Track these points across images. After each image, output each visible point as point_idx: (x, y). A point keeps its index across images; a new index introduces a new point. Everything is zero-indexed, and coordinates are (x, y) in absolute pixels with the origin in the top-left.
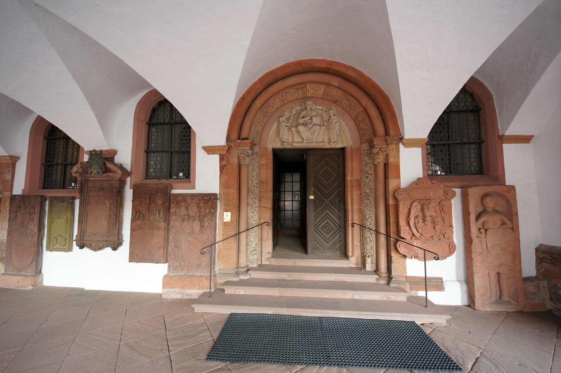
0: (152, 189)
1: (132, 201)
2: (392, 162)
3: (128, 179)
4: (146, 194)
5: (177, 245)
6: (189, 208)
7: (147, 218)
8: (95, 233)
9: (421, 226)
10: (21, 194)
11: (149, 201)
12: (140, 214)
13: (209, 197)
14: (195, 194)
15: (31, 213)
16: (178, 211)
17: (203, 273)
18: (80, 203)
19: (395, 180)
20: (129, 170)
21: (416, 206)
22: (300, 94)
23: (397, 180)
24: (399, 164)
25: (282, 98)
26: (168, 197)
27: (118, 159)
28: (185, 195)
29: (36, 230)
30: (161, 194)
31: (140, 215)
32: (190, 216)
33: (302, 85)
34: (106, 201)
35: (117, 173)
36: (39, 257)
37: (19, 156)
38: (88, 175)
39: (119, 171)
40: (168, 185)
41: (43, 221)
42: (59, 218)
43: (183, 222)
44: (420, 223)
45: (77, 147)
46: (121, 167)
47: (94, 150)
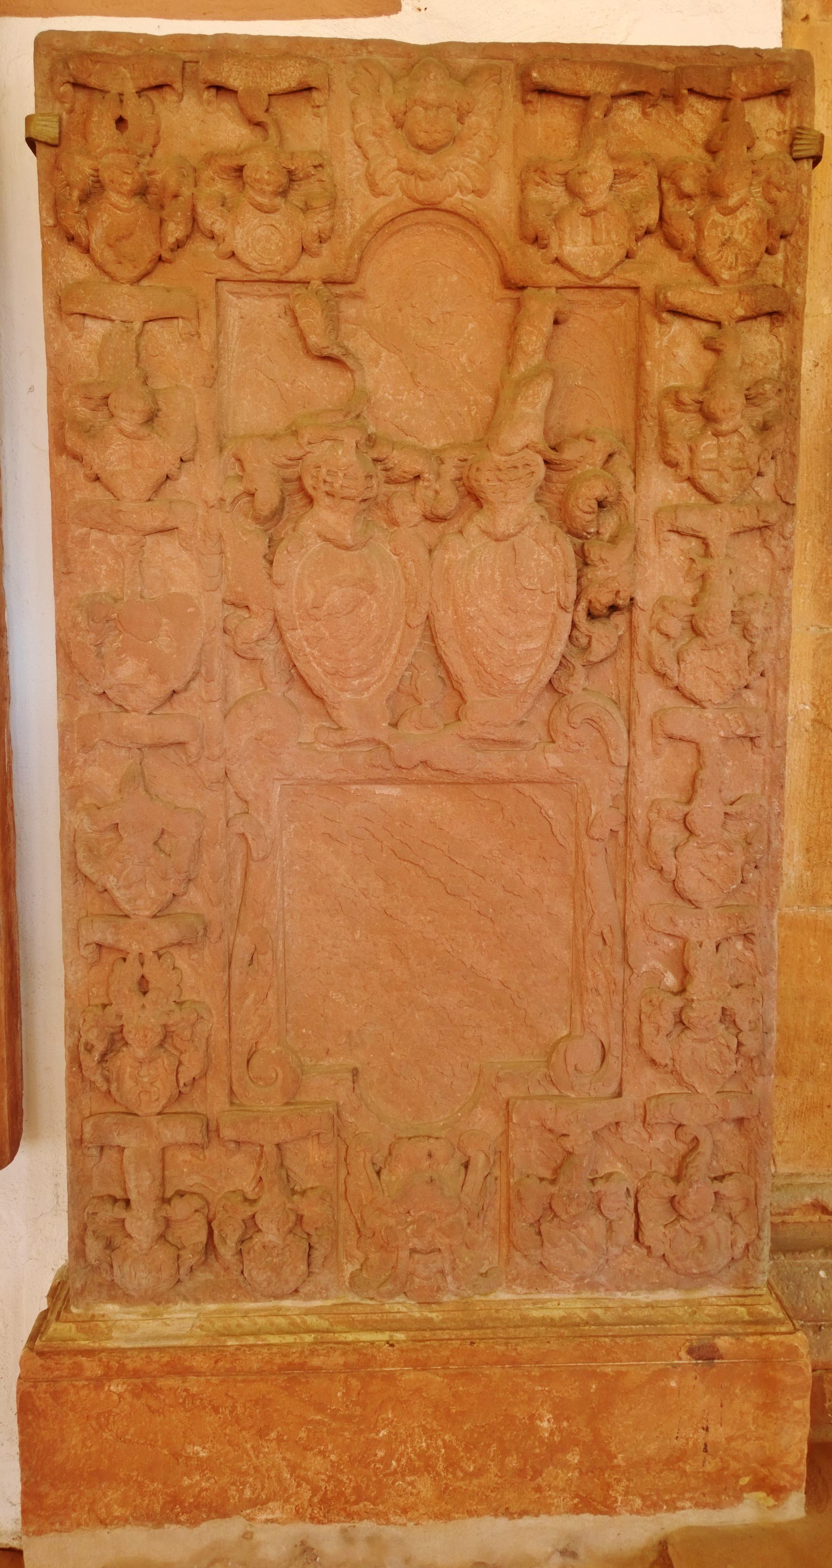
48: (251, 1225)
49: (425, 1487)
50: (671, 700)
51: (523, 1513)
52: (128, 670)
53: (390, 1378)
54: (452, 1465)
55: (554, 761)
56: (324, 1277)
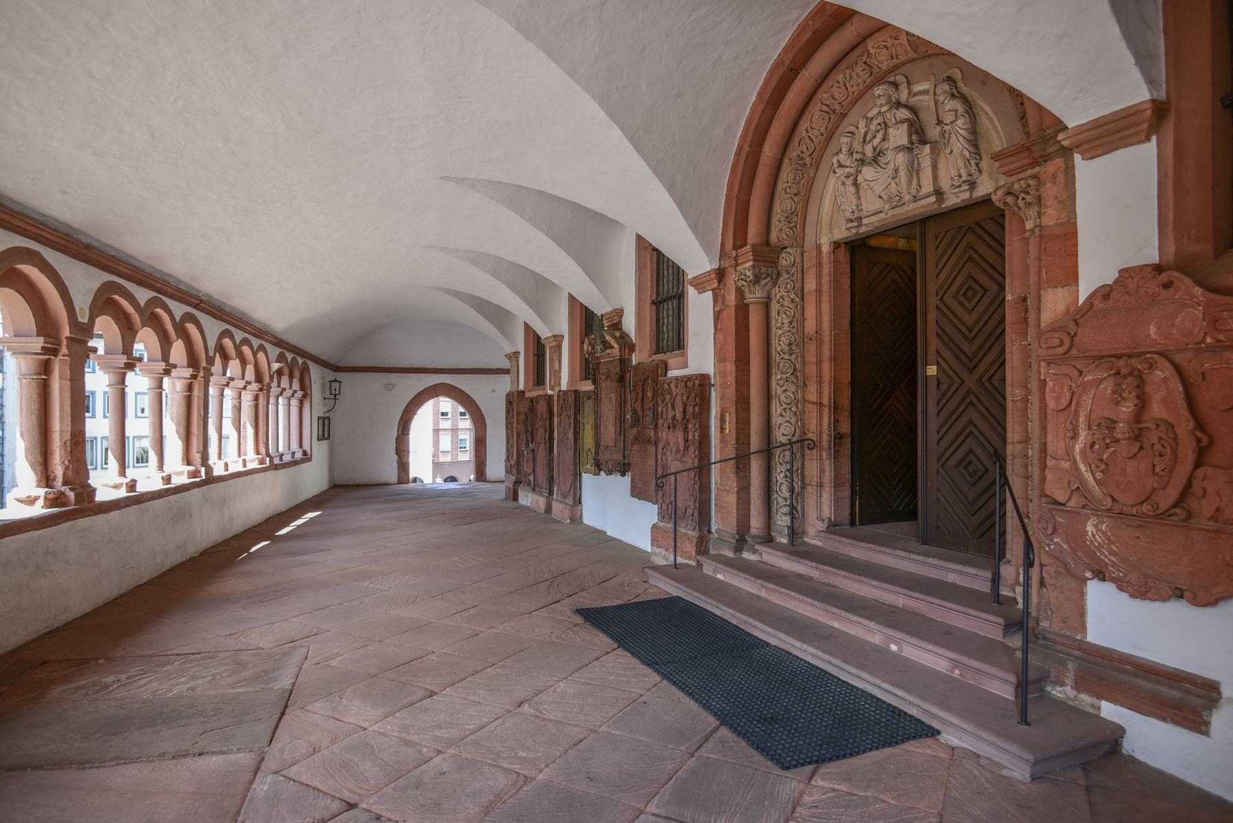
2: (1052, 223)
9: (1105, 457)
19: (1060, 289)
21: (1101, 381)
22: (860, 75)
23: (1066, 288)
24: (1075, 224)
25: (824, 108)
33: (859, 50)
44: (1097, 447)
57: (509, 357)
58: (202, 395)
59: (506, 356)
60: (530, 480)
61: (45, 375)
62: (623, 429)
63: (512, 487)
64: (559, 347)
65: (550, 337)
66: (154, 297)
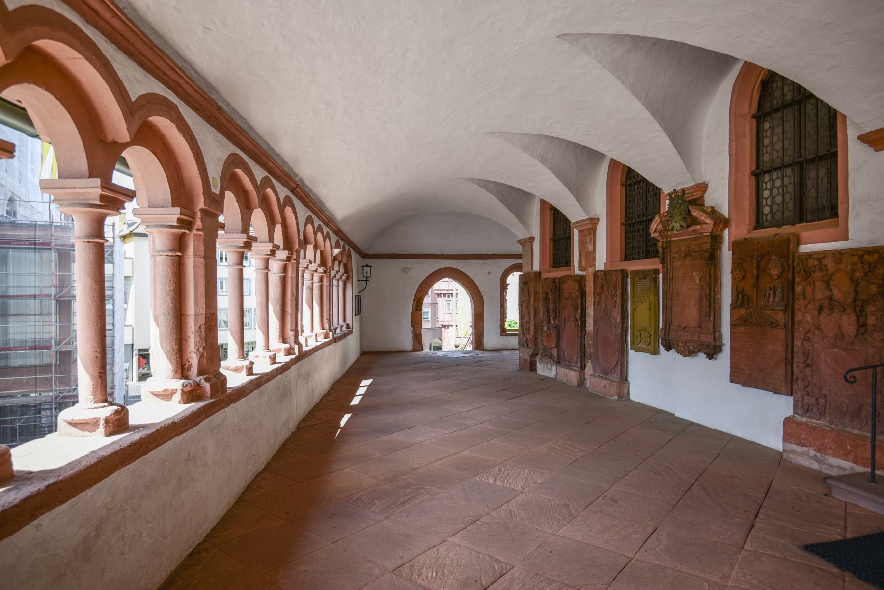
0: (762, 247)
1: (731, 273)
3: (726, 233)
4: (752, 257)
5: (809, 361)
6: (831, 283)
7: (755, 303)
8: (682, 328)
10: (603, 269)
11: (758, 271)
12: (744, 296)
13: (876, 256)
14: (845, 251)
15: (613, 295)
16: (809, 289)
17: (865, 432)
18: (663, 278)
20: (727, 216)
26: (790, 262)
27: (710, 199)
28: (822, 255)
29: (619, 320)
30: (776, 255)
31: (743, 297)
32: (835, 301)
34: (694, 274)
35: (706, 223)
36: (624, 358)
37: (598, 217)
38: (669, 233)
39: (708, 220)
40: (791, 236)
41: (626, 307)
42: (642, 302)
43: (820, 314)
45: (657, 191)
46: (713, 213)
47: (675, 190)
48: (812, 409)
49: (831, 451)
50: (873, 340)
51: (845, 460)
52: (801, 329)
53: (827, 433)
54: (835, 449)
55: (857, 348)
56: (822, 419)
57: (522, 242)
58: (294, 276)
59: (518, 241)
60: (552, 354)
61: (180, 251)
62: (712, 310)
63: (529, 359)
64: (593, 231)
65: (586, 220)
66: (266, 176)
